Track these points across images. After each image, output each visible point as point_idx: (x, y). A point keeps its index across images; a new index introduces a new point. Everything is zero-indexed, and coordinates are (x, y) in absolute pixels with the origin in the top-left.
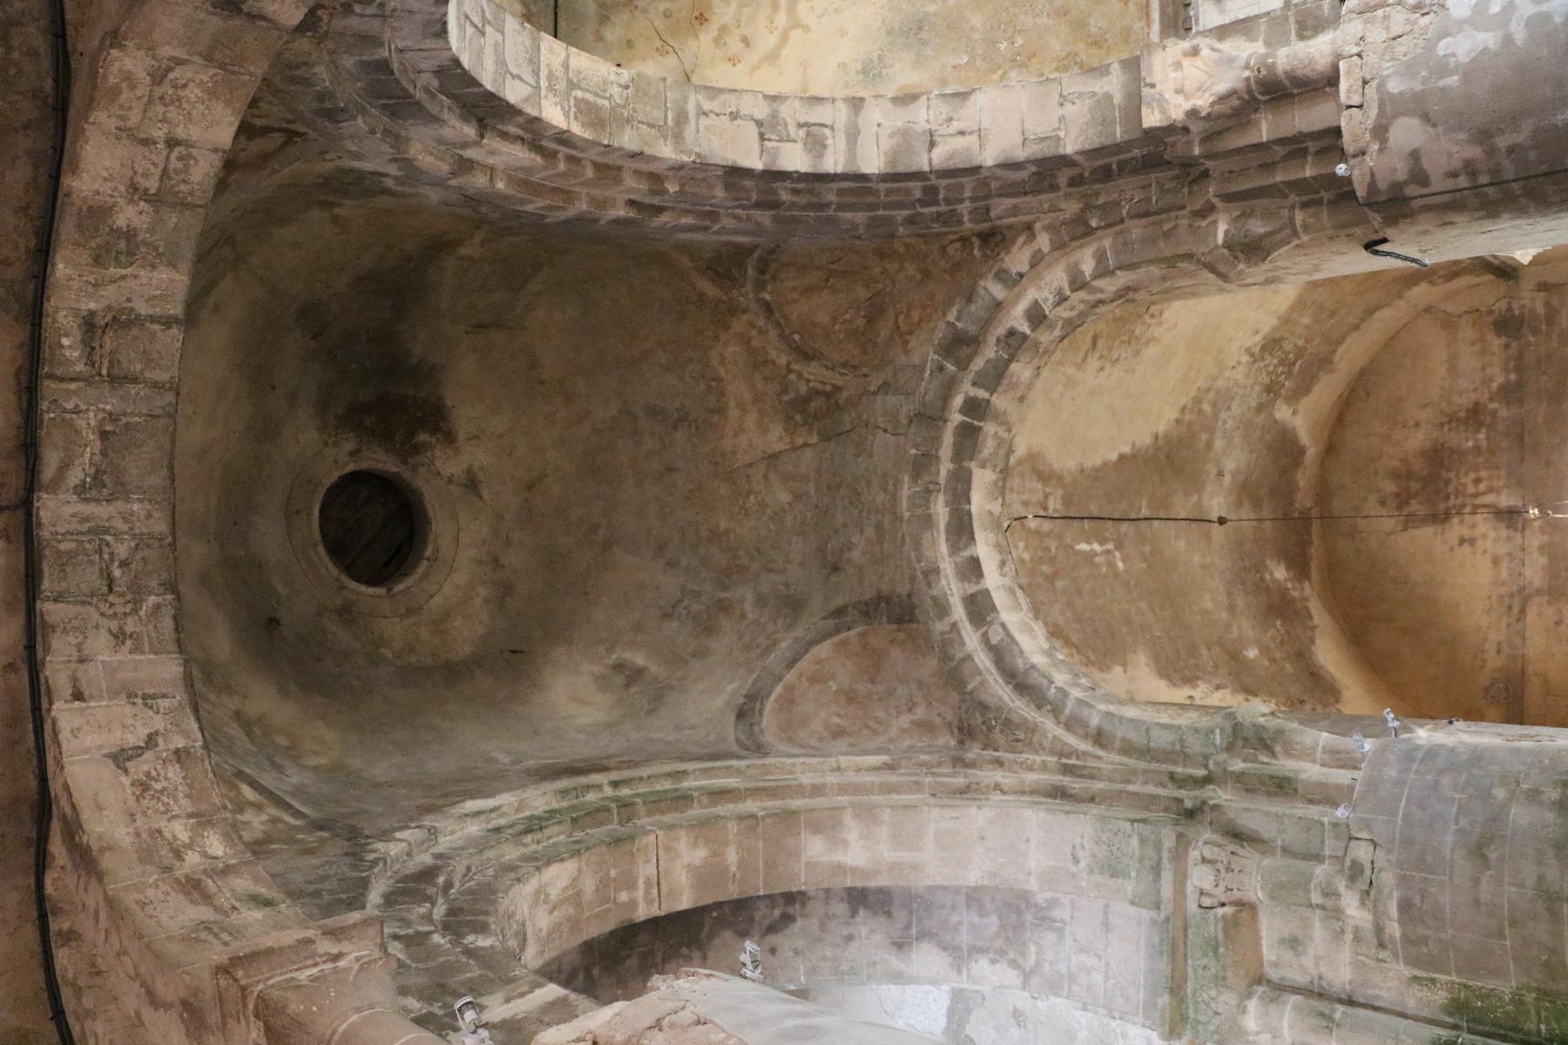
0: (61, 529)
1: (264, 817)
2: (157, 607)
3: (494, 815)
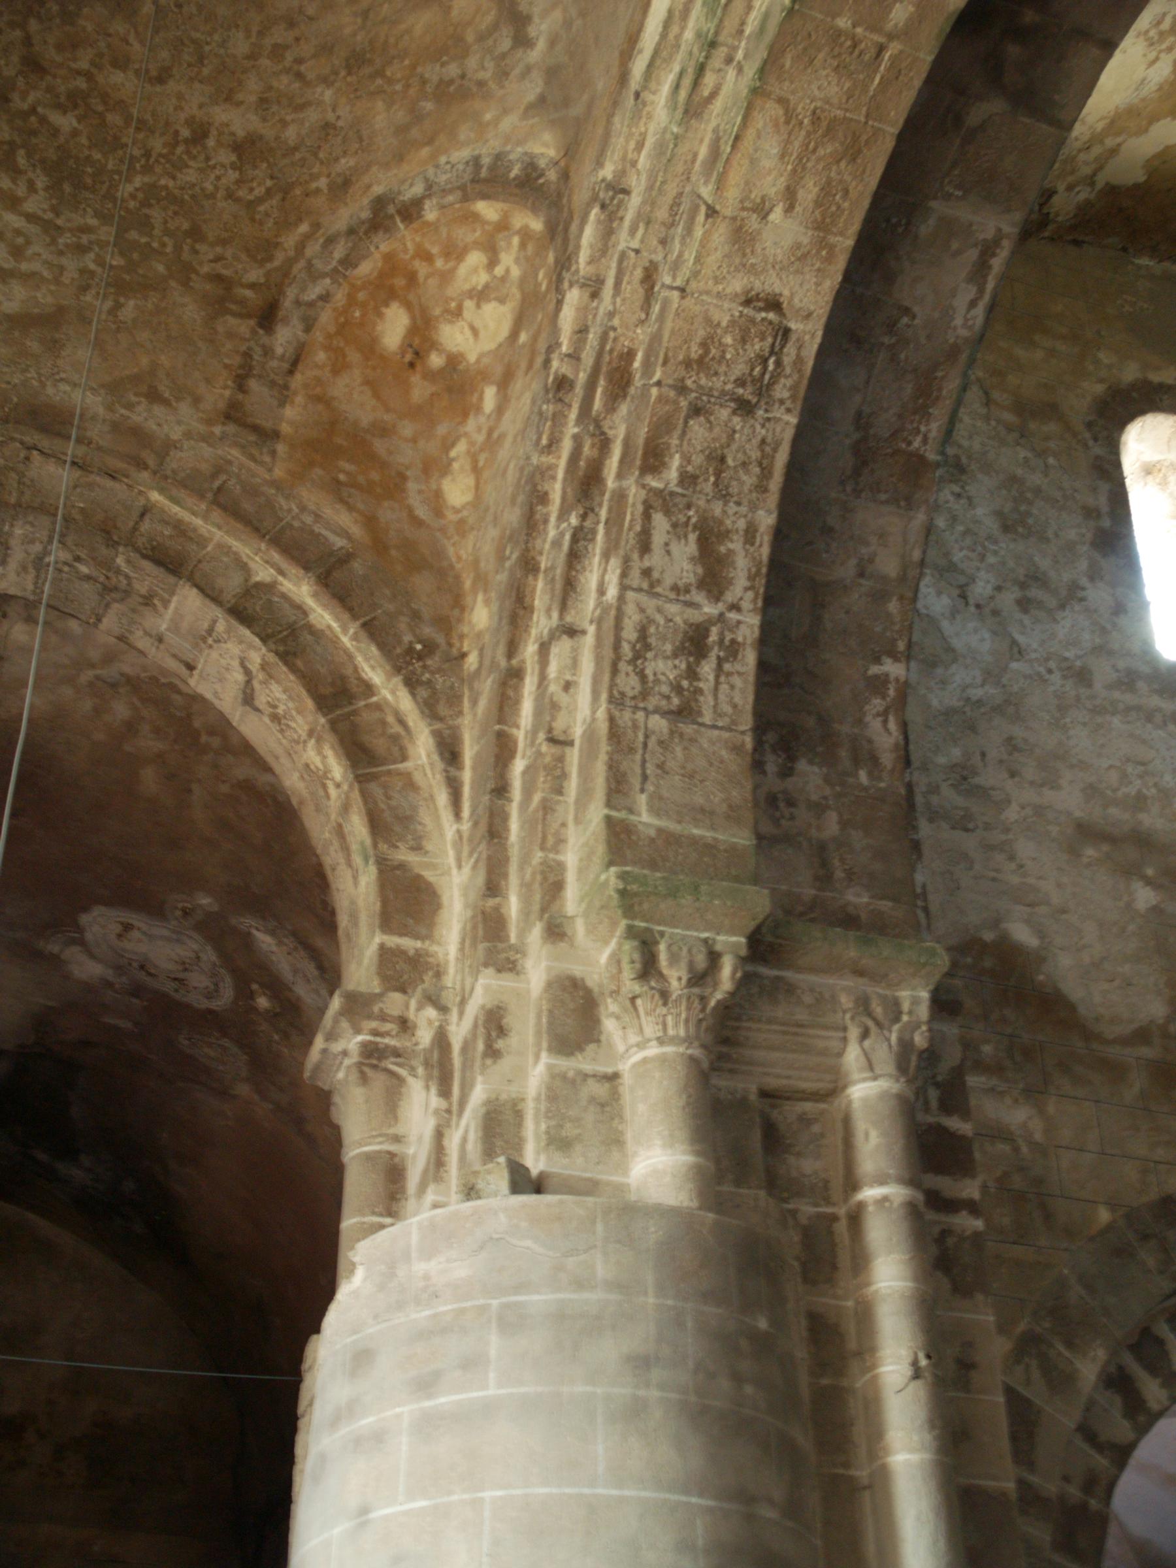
0: (30, 587)
1: (516, 240)
2: (128, 562)
3: (675, 30)
